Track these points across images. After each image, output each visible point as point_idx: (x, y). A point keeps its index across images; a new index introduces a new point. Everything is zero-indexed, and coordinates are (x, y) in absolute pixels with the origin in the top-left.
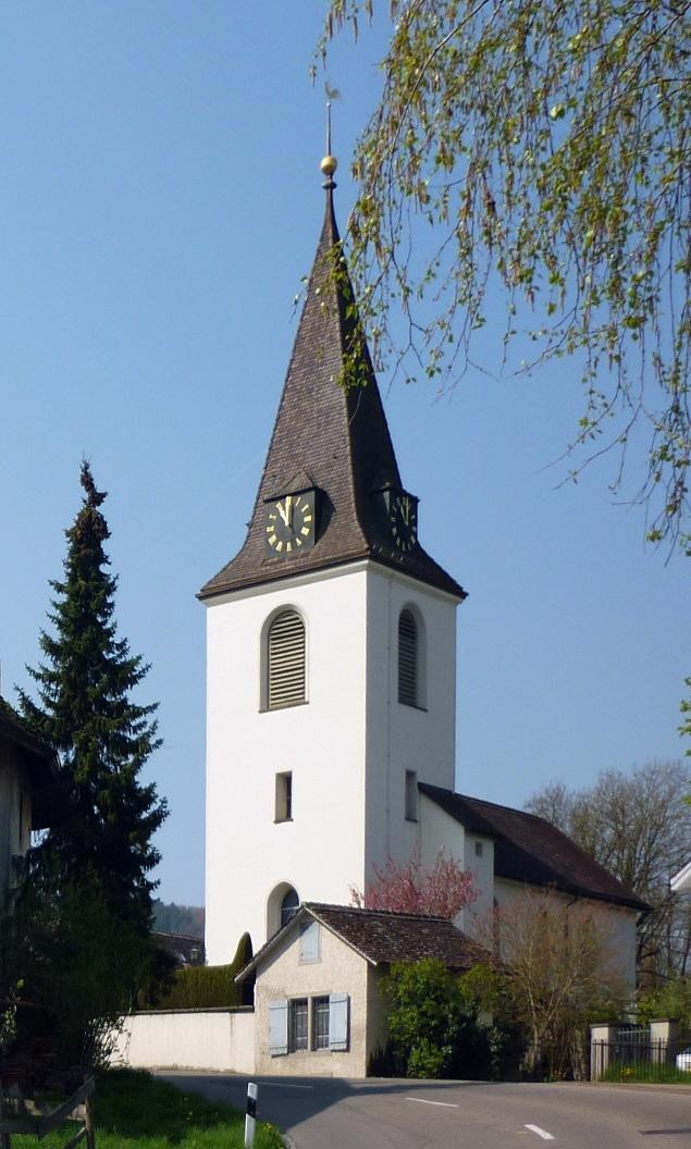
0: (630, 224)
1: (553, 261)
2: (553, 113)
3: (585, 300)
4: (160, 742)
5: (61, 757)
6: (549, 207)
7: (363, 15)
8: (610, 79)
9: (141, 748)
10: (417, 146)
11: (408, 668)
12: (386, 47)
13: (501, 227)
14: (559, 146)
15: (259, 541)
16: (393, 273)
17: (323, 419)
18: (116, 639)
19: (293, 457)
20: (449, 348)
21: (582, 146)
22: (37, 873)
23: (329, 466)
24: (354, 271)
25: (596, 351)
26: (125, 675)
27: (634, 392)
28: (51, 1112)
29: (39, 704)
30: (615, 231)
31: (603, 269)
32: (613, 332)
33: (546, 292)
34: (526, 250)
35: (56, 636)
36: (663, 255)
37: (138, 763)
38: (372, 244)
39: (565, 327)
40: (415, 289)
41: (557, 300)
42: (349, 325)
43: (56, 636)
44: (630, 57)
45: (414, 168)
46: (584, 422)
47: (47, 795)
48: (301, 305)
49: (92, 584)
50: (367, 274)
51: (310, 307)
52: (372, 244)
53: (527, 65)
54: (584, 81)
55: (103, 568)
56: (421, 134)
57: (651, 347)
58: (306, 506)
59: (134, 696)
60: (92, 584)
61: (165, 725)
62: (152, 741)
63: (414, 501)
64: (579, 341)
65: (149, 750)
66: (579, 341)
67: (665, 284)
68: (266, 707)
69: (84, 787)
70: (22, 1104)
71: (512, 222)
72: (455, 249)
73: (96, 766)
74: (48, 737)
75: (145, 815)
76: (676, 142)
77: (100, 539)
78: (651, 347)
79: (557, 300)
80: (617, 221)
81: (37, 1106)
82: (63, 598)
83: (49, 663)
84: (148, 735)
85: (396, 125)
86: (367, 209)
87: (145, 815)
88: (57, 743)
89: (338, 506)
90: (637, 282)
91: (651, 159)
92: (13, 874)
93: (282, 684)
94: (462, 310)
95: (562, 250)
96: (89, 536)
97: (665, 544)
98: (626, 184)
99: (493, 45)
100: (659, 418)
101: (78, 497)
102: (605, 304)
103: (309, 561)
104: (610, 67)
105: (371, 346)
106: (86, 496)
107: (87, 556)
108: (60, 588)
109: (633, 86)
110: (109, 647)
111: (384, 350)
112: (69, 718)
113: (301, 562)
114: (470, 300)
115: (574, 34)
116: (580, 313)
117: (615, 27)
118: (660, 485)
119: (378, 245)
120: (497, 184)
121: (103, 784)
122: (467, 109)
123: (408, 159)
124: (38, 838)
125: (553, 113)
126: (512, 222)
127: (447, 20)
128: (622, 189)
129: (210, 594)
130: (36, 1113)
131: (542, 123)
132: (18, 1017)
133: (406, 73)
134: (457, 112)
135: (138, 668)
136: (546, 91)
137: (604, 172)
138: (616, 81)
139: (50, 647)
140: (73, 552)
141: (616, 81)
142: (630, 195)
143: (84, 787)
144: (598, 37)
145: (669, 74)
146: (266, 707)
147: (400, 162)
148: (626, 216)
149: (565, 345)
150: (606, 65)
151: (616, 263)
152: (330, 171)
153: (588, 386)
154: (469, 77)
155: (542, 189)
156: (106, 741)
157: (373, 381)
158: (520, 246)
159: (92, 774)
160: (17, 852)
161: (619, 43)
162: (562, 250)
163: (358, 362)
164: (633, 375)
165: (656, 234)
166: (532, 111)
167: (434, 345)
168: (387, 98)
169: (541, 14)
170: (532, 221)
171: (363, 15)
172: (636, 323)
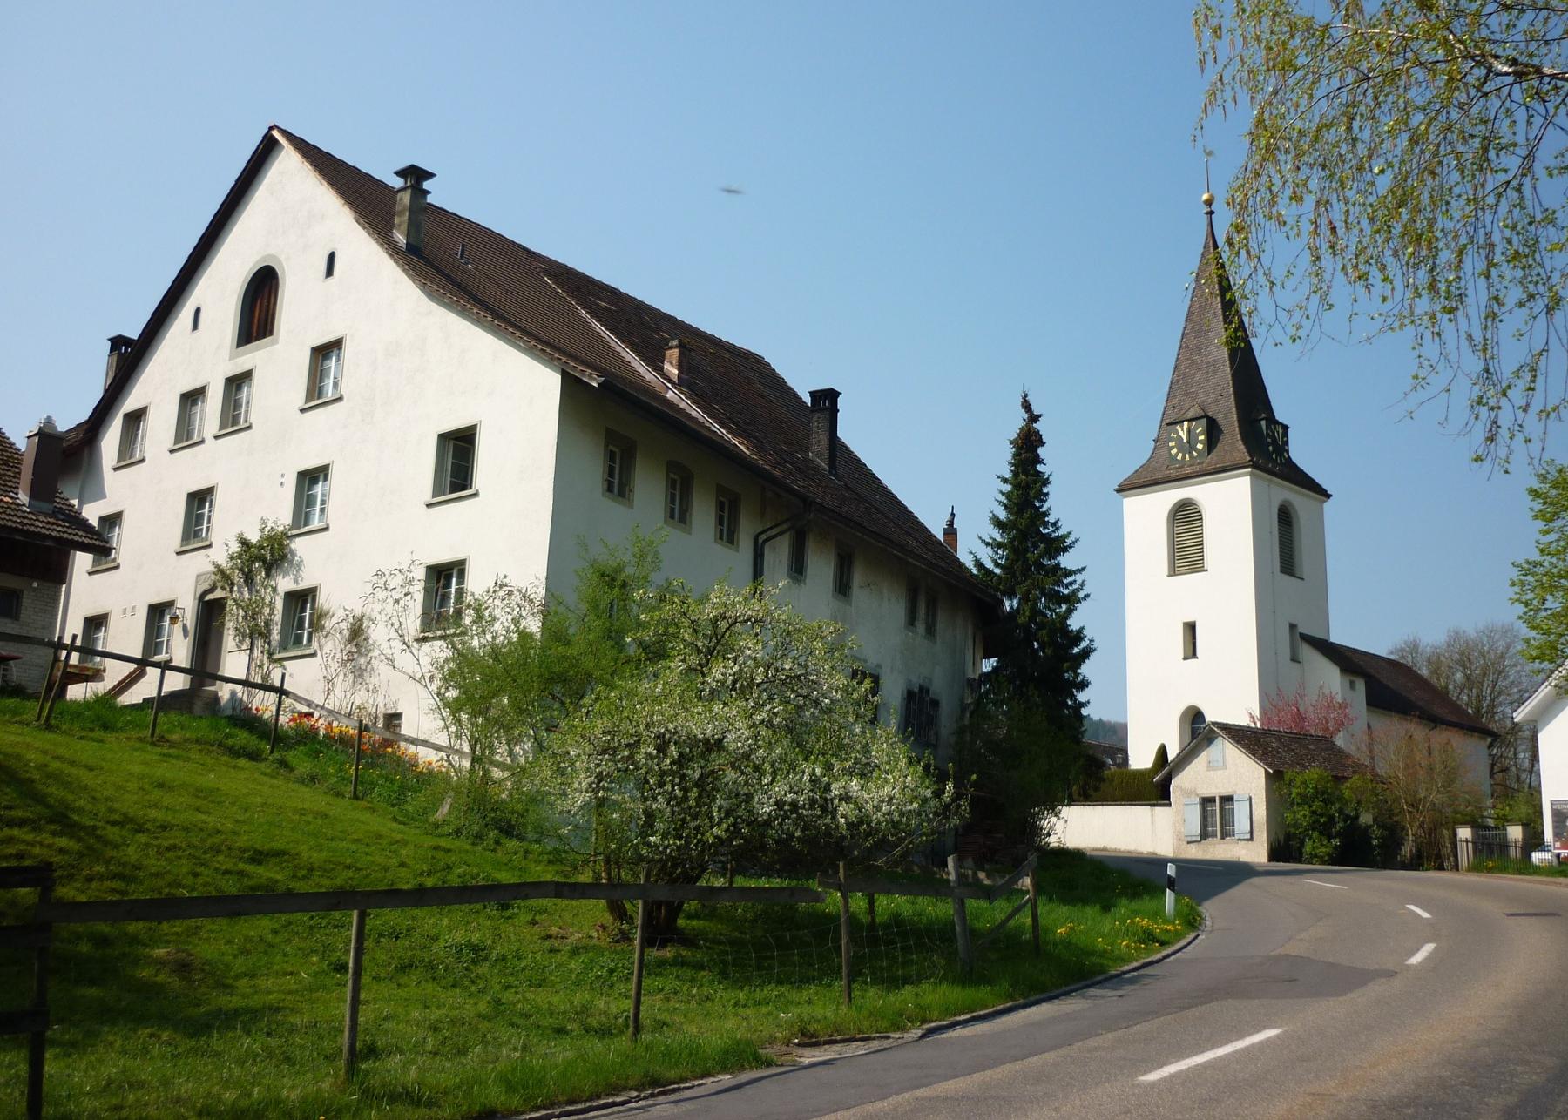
0: (1440, 245)
1: (1383, 268)
2: (1376, 170)
3: (1410, 294)
4: (1087, 596)
5: (1007, 605)
6: (1378, 232)
7: (1230, 104)
8: (1417, 150)
9: (1073, 600)
10: (1275, 189)
11: (1286, 547)
12: (1248, 124)
13: (1342, 243)
14: (1382, 192)
15: (1164, 453)
16: (1261, 271)
17: (1211, 369)
18: (1051, 519)
19: (1188, 394)
20: (1305, 322)
21: (1400, 192)
22: (987, 692)
23: (1217, 401)
24: (1230, 270)
25: (1421, 329)
26: (1059, 545)
27: (1453, 358)
28: (1000, 882)
29: (989, 565)
30: (1429, 248)
31: (1422, 275)
32: (1433, 316)
33: (1379, 288)
34: (1361, 259)
35: (1002, 515)
36: (1468, 265)
37: (1070, 611)
38: (1243, 252)
39: (1396, 311)
40: (1279, 283)
41: (1388, 293)
42: (1229, 306)
43: (1002, 515)
44: (1432, 137)
45: (1273, 203)
46: (1416, 377)
47: (994, 632)
48: (1190, 291)
49: (1030, 479)
50: (1240, 271)
51: (1198, 292)
52: (1243, 252)
53: (1355, 140)
54: (1398, 151)
55: (1040, 468)
56: (1276, 179)
57: (1463, 327)
58: (1200, 429)
59: (1066, 561)
60: (1030, 479)
61: (1091, 582)
62: (1081, 595)
63: (1285, 428)
64: (1407, 321)
65: (1079, 602)
66: (1407, 321)
67: (1471, 285)
68: (1173, 572)
69: (1026, 628)
70: (975, 874)
71: (1350, 241)
72: (1307, 257)
73: (1036, 612)
74: (997, 589)
75: (1076, 650)
76: (1471, 192)
77: (1036, 448)
78: (1463, 327)
79: (1388, 293)
80: (1430, 242)
81: (988, 876)
82: (1008, 488)
83: (997, 535)
84: (1077, 590)
85: (1257, 175)
86: (1238, 229)
87: (1076, 650)
88: (1004, 594)
89: (1226, 430)
90: (1449, 284)
91: (1453, 202)
92: (967, 691)
93: (1186, 554)
94: (1315, 299)
95: (1389, 260)
96: (1028, 445)
97: (1487, 465)
98: (1435, 219)
99: (1328, 126)
100: (1474, 376)
101: (1018, 419)
102: (1426, 297)
103: (1204, 467)
104: (1417, 143)
105: (1246, 320)
106: (1026, 416)
107: (1026, 459)
108: (1005, 481)
109: (1435, 155)
110: (1045, 525)
111: (1257, 323)
112: (1014, 575)
113: (1198, 468)
114: (1322, 292)
115: (1388, 122)
116: (1406, 303)
117: (1418, 119)
118: (1479, 423)
119: (1248, 253)
120: (1337, 213)
121: (1041, 626)
122: (1311, 166)
123: (1269, 196)
124: (988, 665)
125: (1376, 170)
126: (1350, 241)
127: (1292, 110)
128: (1432, 222)
129: (1126, 488)
130: (987, 882)
131: (1369, 177)
132: (971, 804)
133: (1264, 142)
134: (1304, 169)
135: (1069, 541)
136: (1370, 156)
137: (1417, 210)
138: (1422, 152)
139: (997, 523)
140: (1015, 456)
141: (1422, 152)
142: (1439, 225)
143: (1026, 628)
144: (1406, 124)
145: (1461, 148)
146: (1173, 572)
147: (1262, 199)
148: (1437, 239)
149: (1397, 324)
150: (1414, 141)
151: (1432, 270)
152: (1209, 203)
153: (1416, 353)
154: (1311, 145)
155: (1372, 220)
156: (1043, 593)
157: (1249, 345)
158: (1357, 257)
159: (1032, 618)
160: (971, 675)
161: (1423, 128)
162: (1389, 260)
163: (1236, 330)
164: (1451, 344)
165: (1461, 252)
166: (1360, 169)
167: (1295, 319)
168: (1250, 157)
169: (1362, 108)
170: (1365, 241)
171: (1230, 104)
172: (1452, 311)
